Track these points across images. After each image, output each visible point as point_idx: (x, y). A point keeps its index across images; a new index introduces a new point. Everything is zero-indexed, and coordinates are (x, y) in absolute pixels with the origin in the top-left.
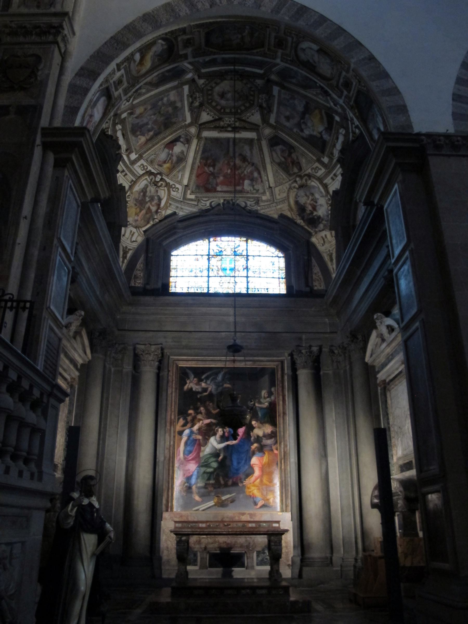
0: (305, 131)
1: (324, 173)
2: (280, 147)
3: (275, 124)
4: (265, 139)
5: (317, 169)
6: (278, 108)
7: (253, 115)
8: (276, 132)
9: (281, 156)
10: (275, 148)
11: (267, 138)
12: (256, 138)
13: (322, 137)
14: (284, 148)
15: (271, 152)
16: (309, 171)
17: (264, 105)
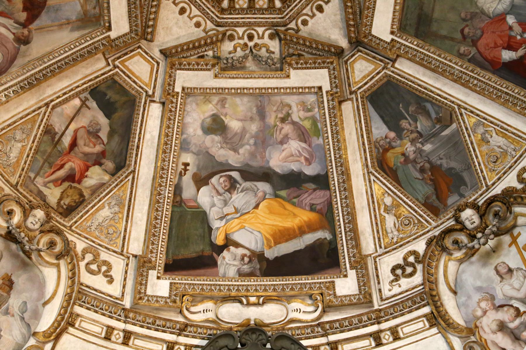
0: (203, 189)
1: (111, 296)
2: (103, 120)
3: (178, 89)
4: (115, 67)
5: (104, 268)
6: (240, 92)
7: (182, 11)
8: (148, 95)
9: (76, 131)
10: (93, 104)
11: (117, 70)
12: (113, 34)
13: (220, 249)
14: (104, 135)
15: (77, 95)
16: (80, 246)
17: (227, 47)
